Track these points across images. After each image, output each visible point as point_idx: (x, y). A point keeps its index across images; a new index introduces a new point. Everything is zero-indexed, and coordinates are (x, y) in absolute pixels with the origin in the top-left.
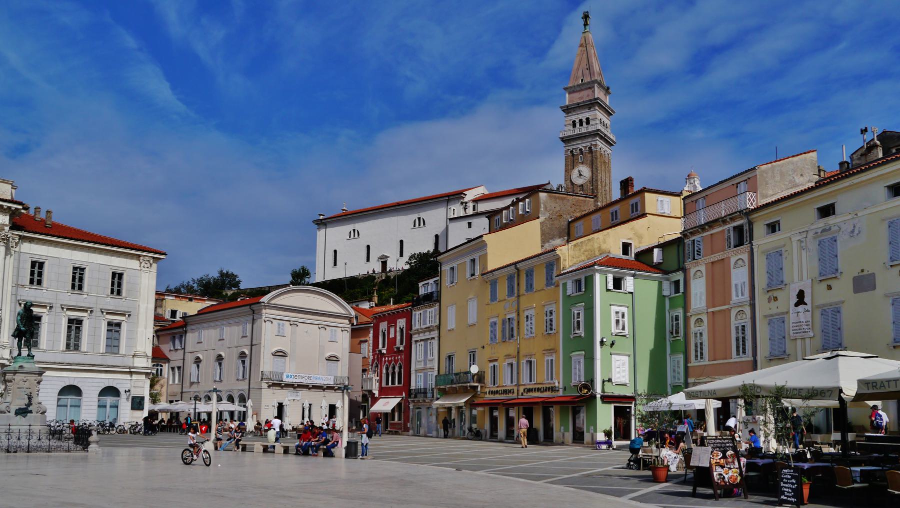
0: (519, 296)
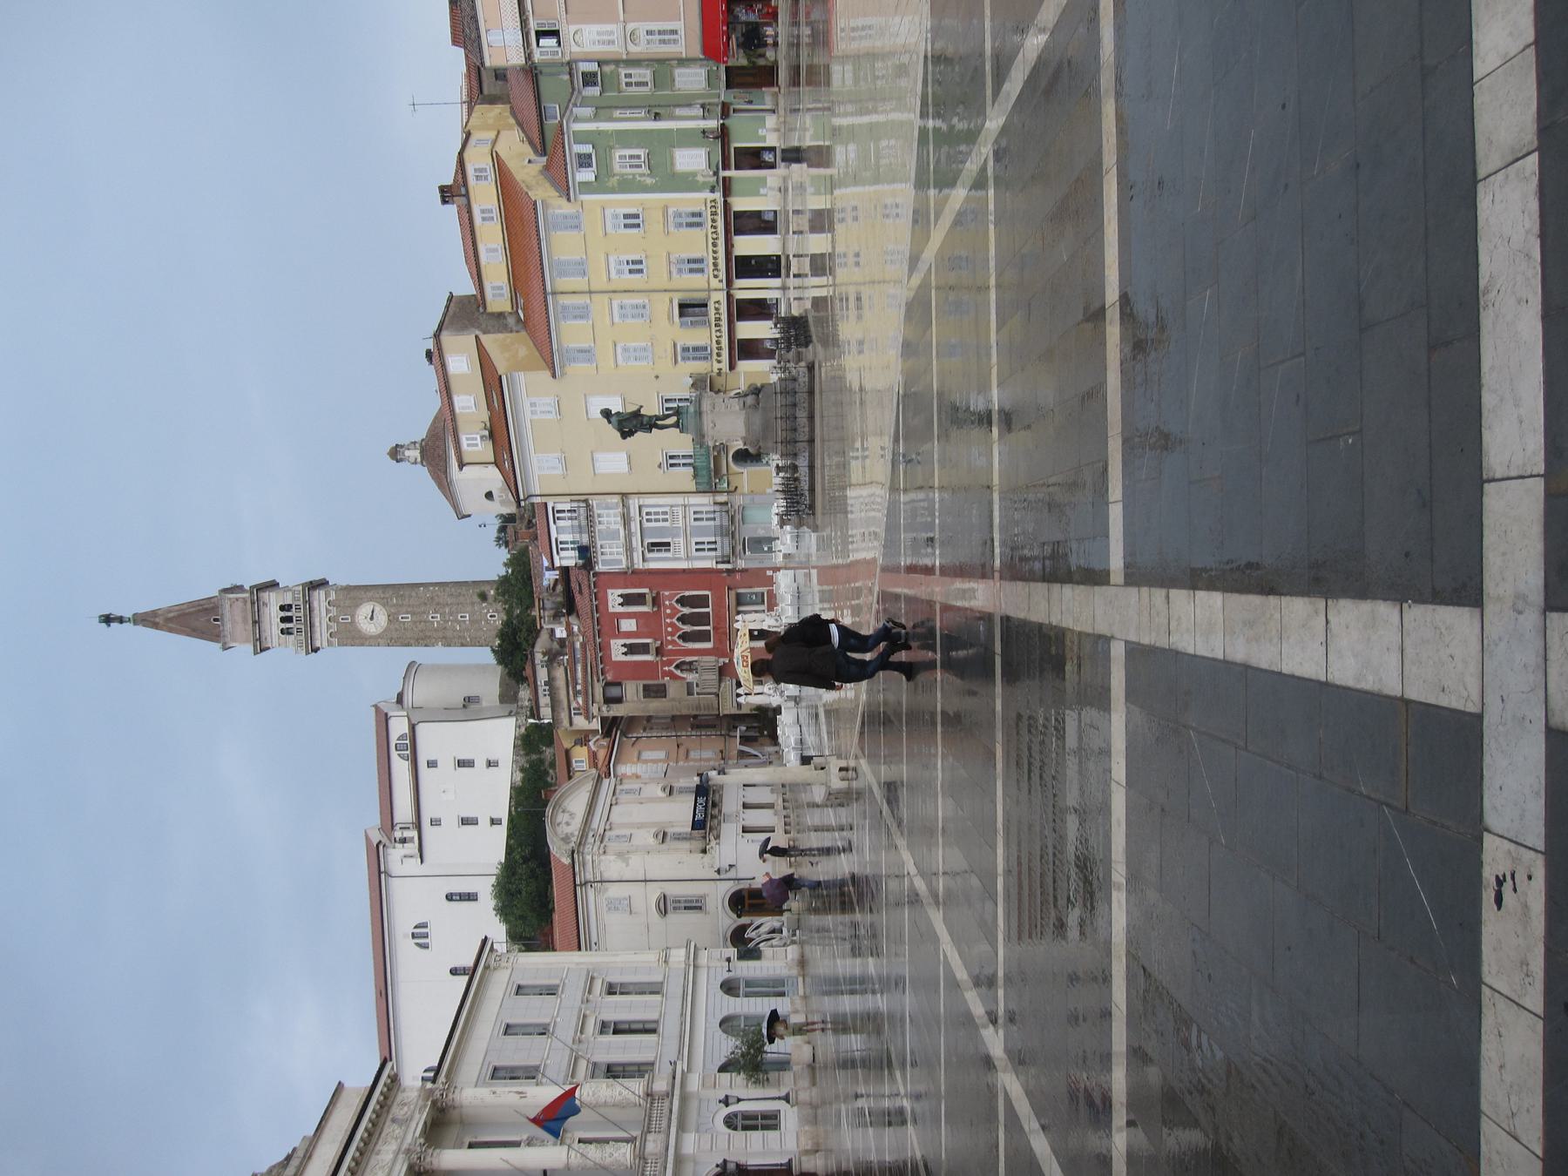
0: (590, 292)
